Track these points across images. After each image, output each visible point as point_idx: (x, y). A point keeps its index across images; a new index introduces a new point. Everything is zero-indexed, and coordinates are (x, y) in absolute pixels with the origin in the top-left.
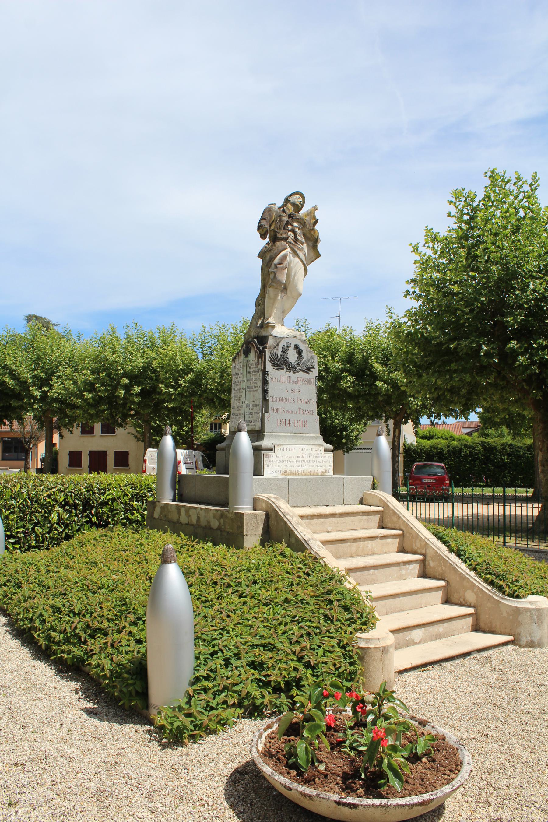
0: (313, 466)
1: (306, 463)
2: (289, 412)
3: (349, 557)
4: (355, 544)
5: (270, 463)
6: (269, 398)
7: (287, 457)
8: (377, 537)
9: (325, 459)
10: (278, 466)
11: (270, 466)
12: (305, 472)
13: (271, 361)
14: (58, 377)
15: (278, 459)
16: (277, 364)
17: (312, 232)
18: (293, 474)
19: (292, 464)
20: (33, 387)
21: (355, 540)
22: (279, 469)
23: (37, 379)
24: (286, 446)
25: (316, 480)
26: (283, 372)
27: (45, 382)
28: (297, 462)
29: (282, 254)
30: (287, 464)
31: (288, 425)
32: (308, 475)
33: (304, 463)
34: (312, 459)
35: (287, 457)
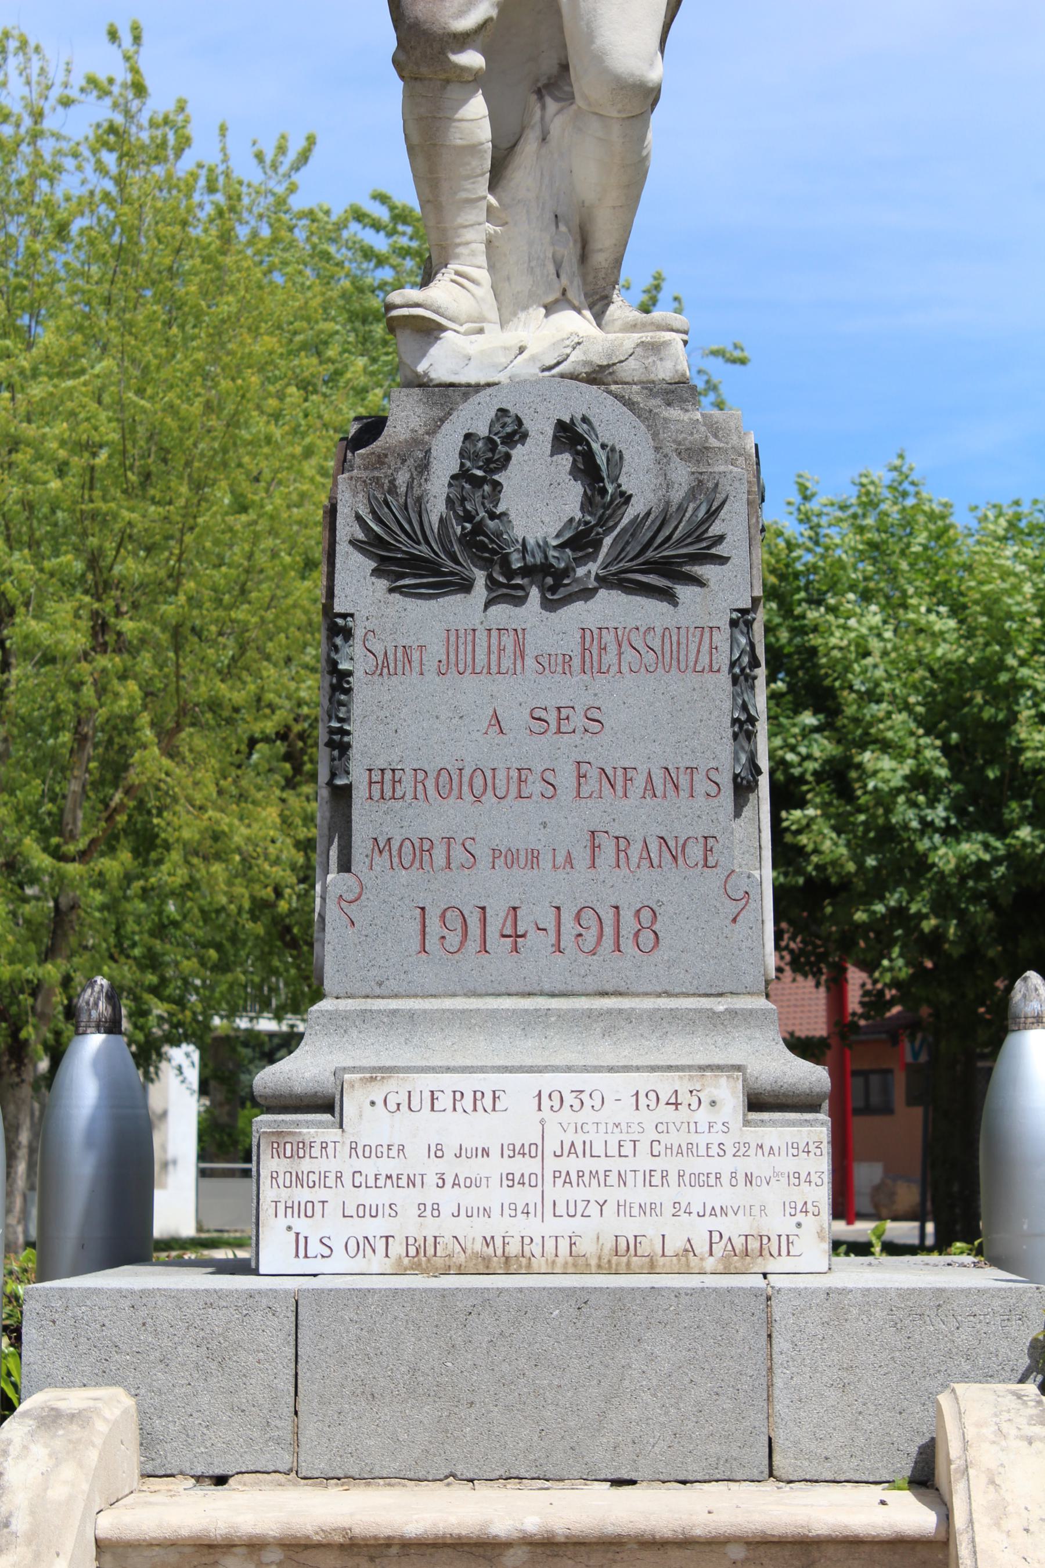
0: (649, 1209)
1: (595, 1192)
5: (303, 1194)
6: (357, 776)
7: (437, 1152)
9: (756, 1164)
10: (364, 1211)
11: (306, 1210)
12: (586, 1246)
13: (372, 545)
15: (369, 1167)
16: (417, 565)
19: (471, 1198)
24: (426, 1082)
25: (528, 1304)
26: (467, 609)
28: (510, 1180)
30: (431, 1195)
31: (499, 946)
33: (578, 1193)
34: (644, 1162)
35: (437, 1152)
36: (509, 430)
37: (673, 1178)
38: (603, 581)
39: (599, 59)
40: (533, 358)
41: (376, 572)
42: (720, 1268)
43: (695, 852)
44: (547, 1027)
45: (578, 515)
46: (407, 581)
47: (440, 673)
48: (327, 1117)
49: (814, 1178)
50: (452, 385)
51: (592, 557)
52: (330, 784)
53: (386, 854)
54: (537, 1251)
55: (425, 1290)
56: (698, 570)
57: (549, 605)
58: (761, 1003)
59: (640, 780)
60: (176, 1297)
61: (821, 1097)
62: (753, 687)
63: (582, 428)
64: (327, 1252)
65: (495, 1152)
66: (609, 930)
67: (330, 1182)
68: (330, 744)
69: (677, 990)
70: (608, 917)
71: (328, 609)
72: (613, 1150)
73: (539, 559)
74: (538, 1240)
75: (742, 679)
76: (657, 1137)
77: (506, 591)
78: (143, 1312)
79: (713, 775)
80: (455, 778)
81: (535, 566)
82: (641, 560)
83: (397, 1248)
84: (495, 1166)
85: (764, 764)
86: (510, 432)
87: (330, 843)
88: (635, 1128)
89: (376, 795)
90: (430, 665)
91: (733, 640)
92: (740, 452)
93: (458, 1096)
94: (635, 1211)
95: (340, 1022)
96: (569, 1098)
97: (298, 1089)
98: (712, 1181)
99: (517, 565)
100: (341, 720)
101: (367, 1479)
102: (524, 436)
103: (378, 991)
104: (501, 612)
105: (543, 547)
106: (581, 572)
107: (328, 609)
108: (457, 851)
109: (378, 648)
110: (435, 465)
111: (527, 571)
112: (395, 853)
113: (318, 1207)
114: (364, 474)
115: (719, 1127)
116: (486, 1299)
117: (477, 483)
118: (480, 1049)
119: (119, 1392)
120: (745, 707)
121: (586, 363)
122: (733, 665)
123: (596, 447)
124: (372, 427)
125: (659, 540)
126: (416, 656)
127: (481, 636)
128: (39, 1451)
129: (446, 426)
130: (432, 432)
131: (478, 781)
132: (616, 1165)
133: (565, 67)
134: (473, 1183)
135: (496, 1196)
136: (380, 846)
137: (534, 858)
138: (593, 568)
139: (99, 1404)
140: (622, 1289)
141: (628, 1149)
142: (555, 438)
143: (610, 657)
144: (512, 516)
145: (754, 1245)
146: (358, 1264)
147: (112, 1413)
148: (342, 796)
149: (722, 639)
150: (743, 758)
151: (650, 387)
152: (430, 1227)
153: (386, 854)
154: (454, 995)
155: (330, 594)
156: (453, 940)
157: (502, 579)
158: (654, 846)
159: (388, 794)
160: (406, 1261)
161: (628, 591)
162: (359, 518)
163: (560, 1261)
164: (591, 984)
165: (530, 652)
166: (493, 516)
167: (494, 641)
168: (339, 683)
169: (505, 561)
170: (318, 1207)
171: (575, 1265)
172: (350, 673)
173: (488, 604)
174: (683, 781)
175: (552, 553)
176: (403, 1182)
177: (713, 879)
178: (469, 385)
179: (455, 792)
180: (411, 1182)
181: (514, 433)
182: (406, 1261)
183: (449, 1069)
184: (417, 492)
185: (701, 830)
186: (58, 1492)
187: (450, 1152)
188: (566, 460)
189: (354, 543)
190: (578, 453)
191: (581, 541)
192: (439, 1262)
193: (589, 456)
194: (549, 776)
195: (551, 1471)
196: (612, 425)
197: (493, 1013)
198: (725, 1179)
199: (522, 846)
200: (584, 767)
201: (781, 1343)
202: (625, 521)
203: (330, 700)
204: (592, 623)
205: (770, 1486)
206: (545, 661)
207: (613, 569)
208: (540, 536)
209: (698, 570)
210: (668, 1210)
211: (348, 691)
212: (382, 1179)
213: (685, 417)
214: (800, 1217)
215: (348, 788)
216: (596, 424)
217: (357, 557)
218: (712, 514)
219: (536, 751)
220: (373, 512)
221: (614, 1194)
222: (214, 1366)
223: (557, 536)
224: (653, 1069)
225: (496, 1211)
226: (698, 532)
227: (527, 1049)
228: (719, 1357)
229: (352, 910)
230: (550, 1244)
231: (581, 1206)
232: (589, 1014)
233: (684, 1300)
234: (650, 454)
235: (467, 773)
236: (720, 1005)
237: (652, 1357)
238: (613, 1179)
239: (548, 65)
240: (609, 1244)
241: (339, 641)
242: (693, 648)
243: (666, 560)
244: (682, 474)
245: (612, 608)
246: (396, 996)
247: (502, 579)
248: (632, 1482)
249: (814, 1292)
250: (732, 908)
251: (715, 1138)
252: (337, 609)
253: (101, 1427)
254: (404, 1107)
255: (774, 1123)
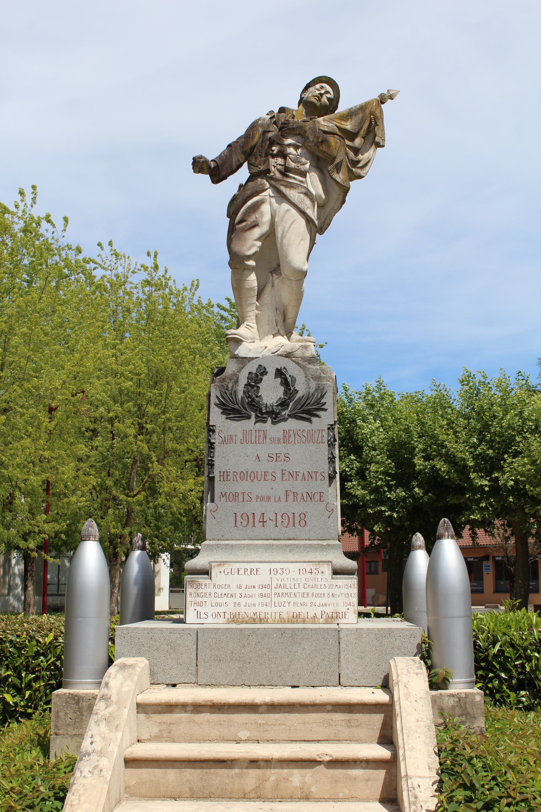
0: (303, 604)
1: (287, 599)
2: (261, 498)
3: (238, 799)
4: (253, 773)
5: (199, 599)
6: (216, 474)
7: (240, 587)
8: (320, 763)
9: (335, 591)
11: (200, 604)
12: (284, 615)
13: (220, 404)
14: (516, 454)
15: (219, 591)
16: (234, 411)
17: (324, 148)
18: (253, 621)
19: (250, 601)
20: (474, 472)
21: (254, 763)
22: (221, 610)
23: (483, 459)
24: (236, 566)
25: (266, 633)
26: (249, 424)
27: (491, 465)
29: (255, 199)
30: (238, 600)
32: (290, 622)
33: (282, 599)
34: (302, 590)
35: (240, 587)
36: (262, 371)
37: (310, 595)
38: (290, 416)
39: (289, 263)
40: (269, 350)
41: (222, 413)
42: (325, 622)
43: (317, 497)
44: (273, 549)
45: (282, 396)
46: (231, 416)
47: (241, 443)
48: (207, 576)
49: (353, 595)
50: (245, 358)
51: (287, 409)
52: (208, 476)
53: (225, 497)
54: (270, 617)
55: (236, 629)
56: (318, 413)
57: (274, 423)
58: (337, 542)
59: (301, 475)
60: (161, 630)
61: (355, 571)
62: (334, 448)
63: (284, 371)
64: (206, 617)
65: (257, 587)
66: (291, 520)
67: (207, 596)
68: (208, 464)
69: (312, 538)
70: (291, 516)
71: (208, 424)
72: (292, 586)
73: (271, 409)
74: (270, 613)
75: (331, 445)
76: (305, 582)
77: (261, 419)
78: (151, 635)
79: (322, 474)
80: (245, 474)
81: (269, 411)
82: (301, 410)
83: (227, 616)
84: (257, 591)
85: (338, 470)
86: (262, 372)
87: (208, 494)
88: (299, 580)
89: (222, 479)
90: (238, 441)
91: (329, 434)
92: (331, 378)
93: (246, 570)
94: (299, 605)
95: (210, 548)
96: (279, 571)
97: (198, 568)
98: (322, 596)
99: (264, 411)
100: (211, 457)
101: (218, 685)
102: (266, 373)
103: (222, 538)
104: (259, 425)
105: (272, 406)
106: (283, 413)
107: (208, 424)
108: (246, 496)
109: (223, 436)
110: (240, 382)
111: (267, 413)
112: (227, 497)
113: (204, 603)
114: (219, 384)
115: (324, 579)
116: (254, 631)
117: (252, 387)
118: (253, 556)
119: (144, 659)
120: (332, 454)
121: (285, 351)
122: (328, 441)
123: (288, 376)
124: (222, 370)
125: (306, 404)
126: (234, 438)
127: (253, 432)
128: (120, 676)
129: (244, 370)
130: (239, 371)
131: (252, 475)
132: (293, 591)
133: (279, 265)
134: (250, 596)
135: (257, 600)
136: (223, 495)
137: (269, 499)
138: (287, 412)
139: (138, 662)
140: (295, 628)
141: (297, 586)
142: (276, 373)
143: (292, 439)
144: (263, 397)
145: (335, 615)
146: (216, 620)
147: (142, 665)
148: (211, 480)
149: (325, 433)
150: (332, 469)
151: (304, 359)
152: (238, 610)
153: (225, 497)
154: (245, 540)
155: (209, 420)
156: (245, 523)
157: (260, 415)
158: (305, 495)
159: (225, 479)
160: (230, 620)
161: (297, 419)
162: (217, 397)
163: (276, 620)
164: (286, 536)
165: (268, 437)
166: (257, 396)
167: (257, 434)
168: (211, 446)
169: (261, 410)
170: (204, 603)
171: (281, 621)
172: (214, 443)
173: (255, 423)
174: (314, 476)
175: (275, 407)
176: (229, 596)
177: (323, 505)
178: (250, 358)
179: (245, 479)
180: (232, 596)
181: (264, 372)
182: (230, 620)
183: (243, 562)
184: (234, 389)
185: (319, 490)
186: (125, 689)
187: (243, 587)
188: (279, 380)
189: (216, 404)
190: (282, 378)
191: (283, 404)
192: (240, 620)
193: (286, 379)
194: (273, 474)
195: (273, 683)
196: (293, 370)
197: (256, 545)
198: (326, 595)
199: (265, 495)
200: (284, 471)
201: (343, 645)
202: (296, 398)
203: (208, 451)
204: (286, 428)
205: (339, 688)
206: (272, 440)
207: (293, 412)
208: (271, 402)
209: (318, 413)
210: (309, 605)
211: (214, 448)
212: (223, 595)
213: (314, 367)
214: (349, 607)
215: (213, 477)
216: (288, 369)
217: (217, 409)
218: (322, 396)
219: (270, 466)
220: (221, 395)
221: (293, 600)
222: (172, 651)
223: (276, 403)
224: (304, 562)
225: (257, 605)
226: (318, 401)
227: (267, 556)
228: (324, 649)
229: (215, 514)
230: (273, 615)
231: (283, 603)
232: (285, 545)
233: (314, 632)
234: (304, 379)
235: (249, 473)
236: (325, 543)
237: (304, 649)
238: (292, 595)
239: (274, 265)
240: (291, 615)
241: (211, 433)
242: (317, 436)
243: (308, 410)
244: (313, 384)
245: (292, 424)
246: (228, 540)
247: (260, 415)
248: (298, 687)
249: (353, 629)
250: (328, 514)
251: (323, 583)
252: (211, 424)
253: (138, 669)
254: (230, 573)
255: (341, 578)
